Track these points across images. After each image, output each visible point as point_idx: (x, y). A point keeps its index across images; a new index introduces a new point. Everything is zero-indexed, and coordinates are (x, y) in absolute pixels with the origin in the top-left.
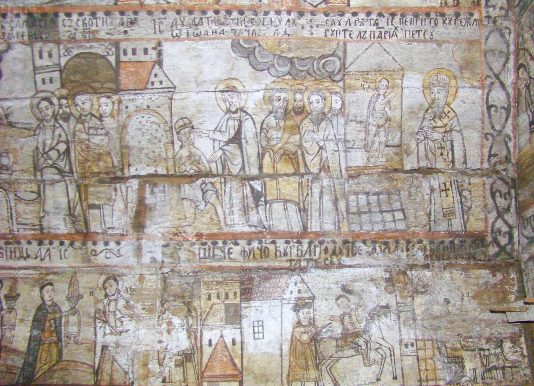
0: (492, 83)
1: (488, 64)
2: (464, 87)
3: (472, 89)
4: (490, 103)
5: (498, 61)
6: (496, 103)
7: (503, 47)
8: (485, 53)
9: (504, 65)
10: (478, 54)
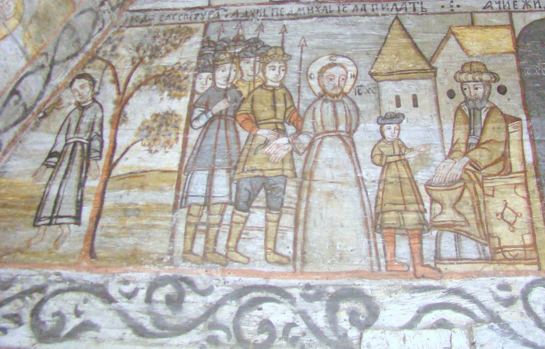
0: (43, 67)
1: (58, 41)
2: (16, 42)
3: (20, 52)
4: (20, 88)
5: (68, 48)
6: (24, 94)
7: (84, 37)
8: (68, 26)
9: (68, 58)
10: (60, 19)
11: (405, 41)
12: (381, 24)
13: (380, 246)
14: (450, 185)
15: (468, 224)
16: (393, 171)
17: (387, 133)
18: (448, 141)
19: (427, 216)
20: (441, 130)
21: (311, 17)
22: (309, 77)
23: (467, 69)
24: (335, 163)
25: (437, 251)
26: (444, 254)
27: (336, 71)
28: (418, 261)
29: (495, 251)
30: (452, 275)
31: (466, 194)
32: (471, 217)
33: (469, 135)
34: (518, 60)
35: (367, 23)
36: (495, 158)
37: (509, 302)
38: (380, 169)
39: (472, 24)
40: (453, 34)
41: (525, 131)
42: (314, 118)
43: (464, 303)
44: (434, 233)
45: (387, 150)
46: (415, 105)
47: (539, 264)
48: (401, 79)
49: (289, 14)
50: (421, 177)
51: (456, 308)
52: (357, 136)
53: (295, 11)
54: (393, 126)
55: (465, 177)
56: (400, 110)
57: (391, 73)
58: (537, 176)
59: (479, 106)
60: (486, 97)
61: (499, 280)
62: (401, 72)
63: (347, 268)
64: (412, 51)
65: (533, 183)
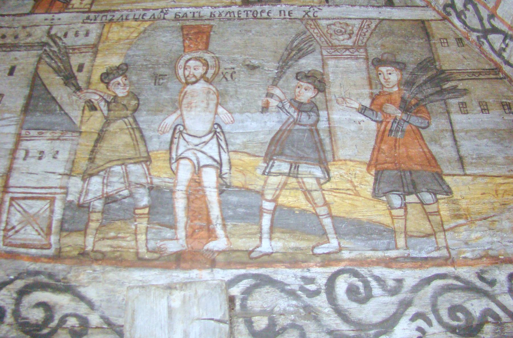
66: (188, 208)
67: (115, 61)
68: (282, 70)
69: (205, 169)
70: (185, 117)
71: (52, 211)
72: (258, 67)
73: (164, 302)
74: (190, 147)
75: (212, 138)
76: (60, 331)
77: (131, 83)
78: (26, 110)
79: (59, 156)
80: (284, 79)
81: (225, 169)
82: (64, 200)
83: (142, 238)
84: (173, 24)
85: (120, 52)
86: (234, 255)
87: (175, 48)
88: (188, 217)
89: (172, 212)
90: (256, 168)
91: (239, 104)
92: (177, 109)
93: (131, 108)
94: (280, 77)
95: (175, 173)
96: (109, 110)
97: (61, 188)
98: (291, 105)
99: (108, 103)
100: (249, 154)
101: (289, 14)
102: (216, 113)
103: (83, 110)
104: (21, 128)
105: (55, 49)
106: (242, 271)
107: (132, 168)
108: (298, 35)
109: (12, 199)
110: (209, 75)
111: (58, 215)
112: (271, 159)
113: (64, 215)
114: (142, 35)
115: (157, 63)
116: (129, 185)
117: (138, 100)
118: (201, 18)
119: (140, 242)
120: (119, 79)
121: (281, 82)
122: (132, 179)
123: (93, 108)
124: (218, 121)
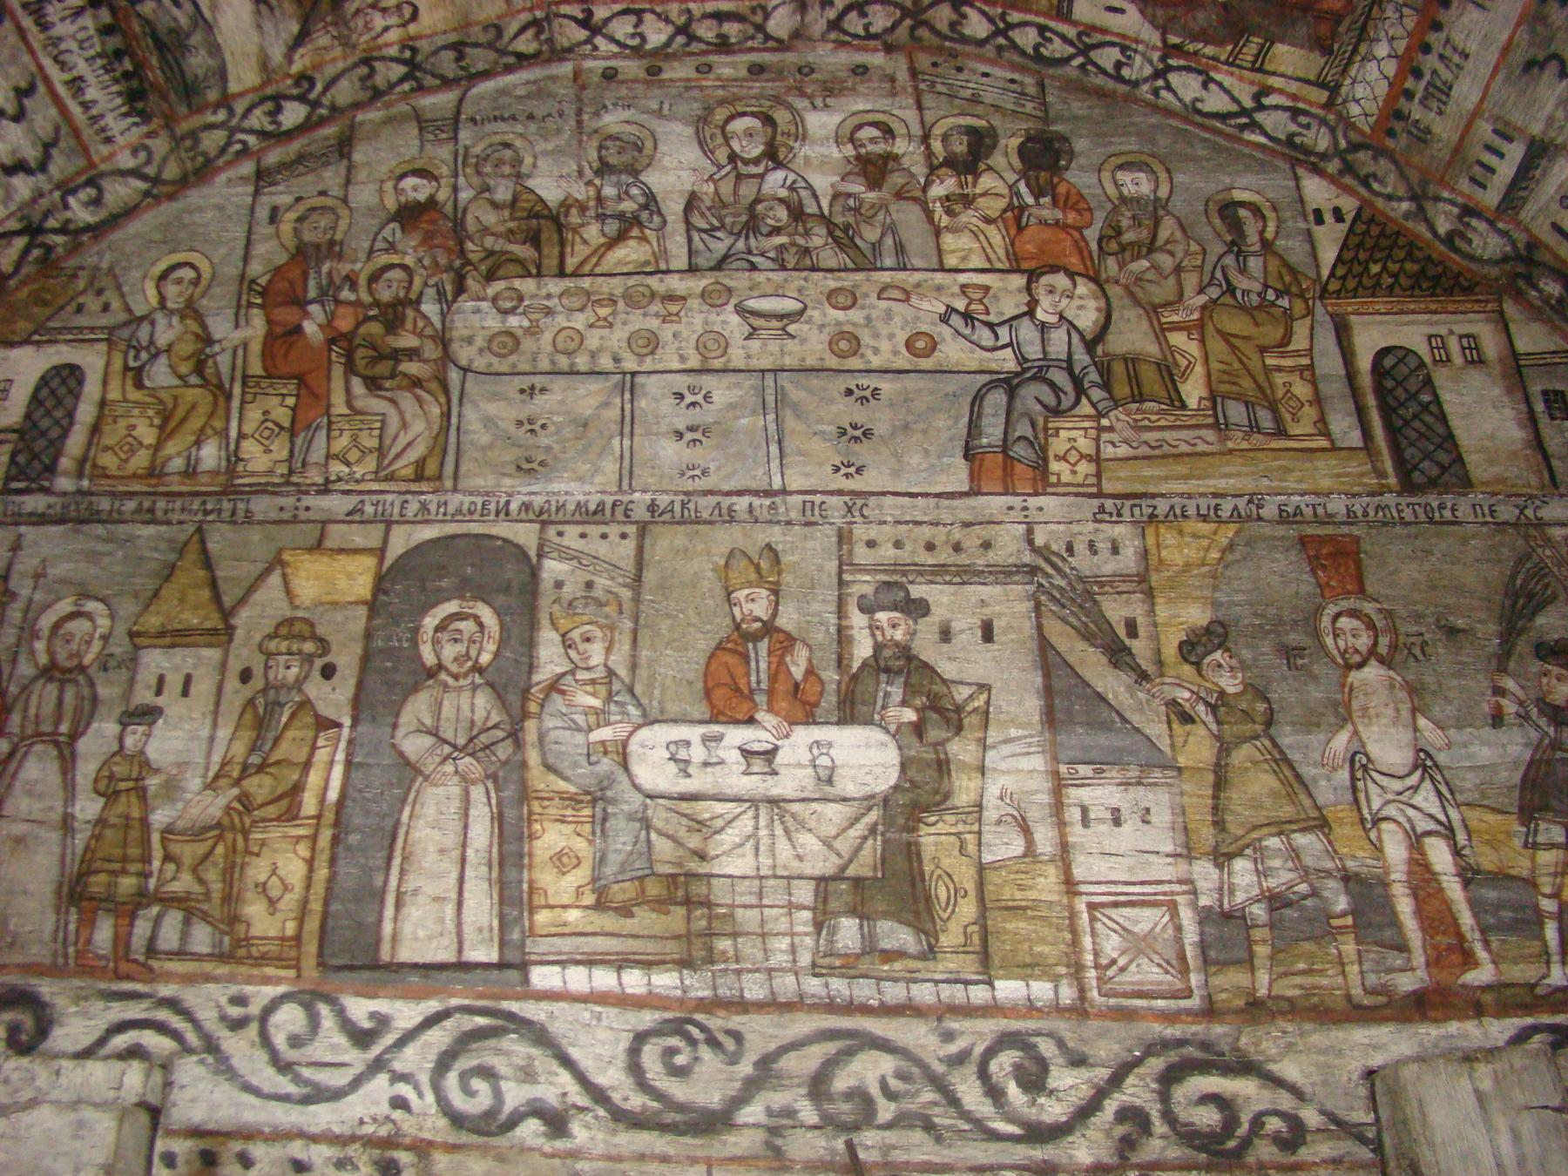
11: (202, 573)
12: (171, 541)
13: (72, 927)
14: (197, 833)
15: (207, 895)
16: (121, 807)
17: (129, 741)
18: (217, 758)
19: (152, 883)
20: (212, 739)
21: (61, 521)
22: (35, 635)
23: (284, 631)
24: (39, 788)
25: (152, 939)
26: (162, 944)
27: (79, 627)
28: (121, 952)
29: (237, 943)
30: (168, 977)
31: (220, 849)
32: (217, 887)
33: (253, 749)
34: (370, 618)
35: (149, 538)
36: (280, 790)
37: (238, 1025)
38: (102, 801)
39: (318, 547)
40: (283, 564)
41: (342, 745)
42: (25, 710)
43: (176, 1022)
44: (155, 910)
45: (120, 769)
46: (185, 693)
47: (298, 968)
48: (172, 646)
49: (31, 514)
50: (160, 817)
51: (162, 1028)
52: (83, 745)
53: (41, 507)
54: (141, 729)
55: (226, 821)
56: (160, 701)
57: (161, 634)
58: (337, 824)
59: (282, 699)
60: (299, 683)
61: (234, 989)
62: (178, 633)
63: (17, 958)
64: (206, 594)
65: (326, 836)
66: (1419, 912)
67: (1197, 615)
68: (1509, 635)
69: (1428, 840)
70: (1364, 736)
71: (1179, 929)
72: (1464, 631)
73: (1465, 1083)
74: (1390, 796)
75: (1422, 779)
76: (1256, 1141)
77: (1243, 666)
78: (1050, 718)
79: (1153, 818)
80: (1514, 657)
81: (1461, 838)
82: (1194, 904)
83: (1353, 970)
84: (1280, 531)
85: (1198, 593)
86: (1510, 992)
87: (1304, 589)
88: (1423, 930)
89: (1394, 922)
90: (1510, 835)
91: (1451, 710)
92: (1345, 720)
93: (1258, 719)
94: (1508, 654)
95: (1378, 848)
96: (1219, 723)
97: (1180, 882)
98: (1541, 712)
99: (1213, 708)
100: (1494, 810)
101: (1492, 512)
102: (1416, 729)
103: (1169, 723)
104: (1055, 759)
105: (1063, 583)
106: (1529, 1020)
107: (1300, 839)
108: (1520, 561)
109: (1092, 907)
110: (1383, 649)
111: (1191, 935)
112: (1531, 818)
113: (1202, 934)
114: (1230, 557)
115: (1280, 621)
116: (1305, 873)
117: (1267, 700)
118: (1329, 519)
119: (1351, 977)
120: (1217, 655)
121: (1512, 665)
122: (1308, 861)
123: (1187, 718)
124: (1422, 744)
